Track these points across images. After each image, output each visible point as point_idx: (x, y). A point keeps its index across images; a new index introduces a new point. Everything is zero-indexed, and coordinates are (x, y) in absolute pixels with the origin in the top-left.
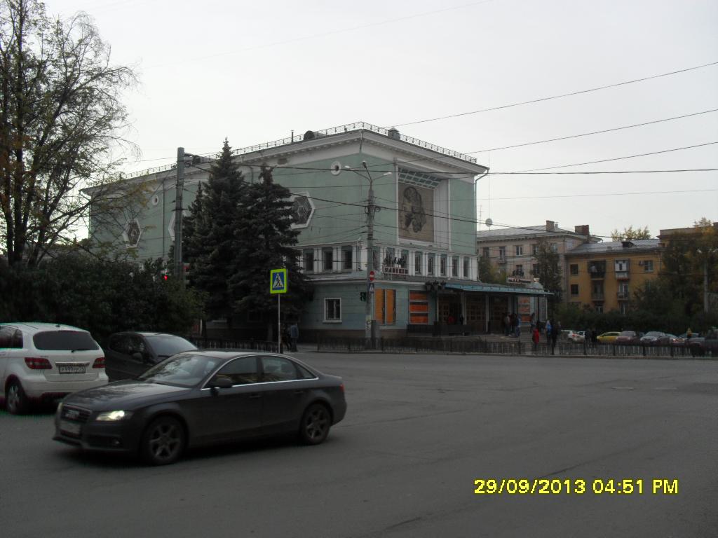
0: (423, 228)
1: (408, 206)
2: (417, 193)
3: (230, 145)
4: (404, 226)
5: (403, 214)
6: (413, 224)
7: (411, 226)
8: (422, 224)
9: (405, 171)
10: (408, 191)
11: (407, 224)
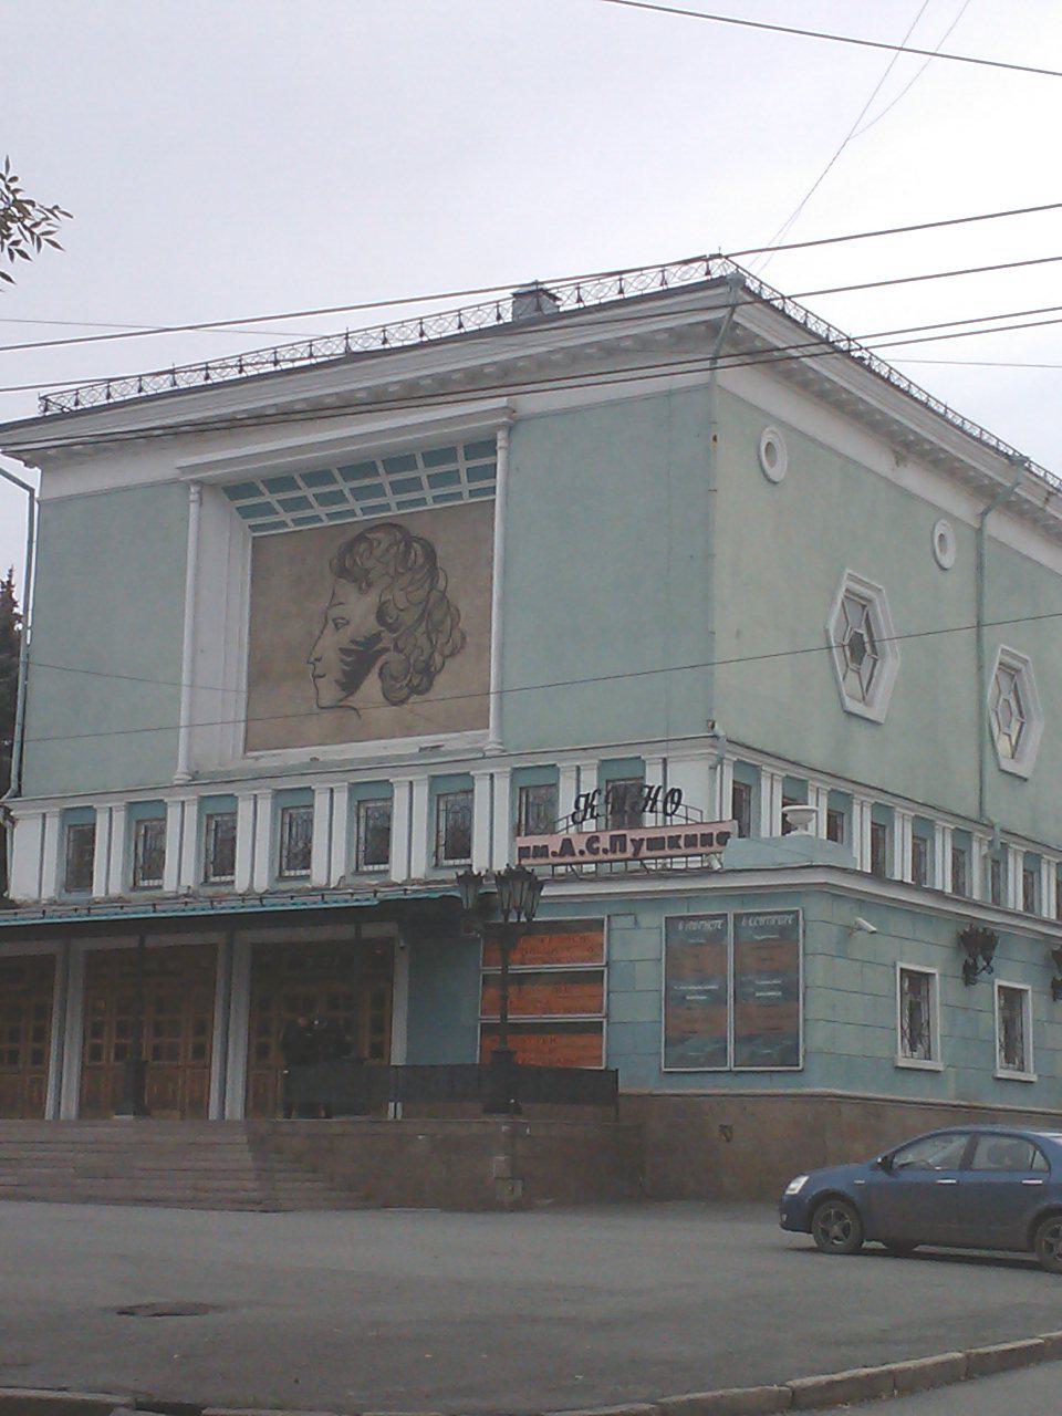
0: (440, 681)
1: (360, 610)
2: (408, 539)
3: (13, 583)
4: (329, 693)
5: (330, 646)
7: (372, 686)
8: (438, 658)
9: (280, 482)
10: (363, 546)
11: (351, 683)
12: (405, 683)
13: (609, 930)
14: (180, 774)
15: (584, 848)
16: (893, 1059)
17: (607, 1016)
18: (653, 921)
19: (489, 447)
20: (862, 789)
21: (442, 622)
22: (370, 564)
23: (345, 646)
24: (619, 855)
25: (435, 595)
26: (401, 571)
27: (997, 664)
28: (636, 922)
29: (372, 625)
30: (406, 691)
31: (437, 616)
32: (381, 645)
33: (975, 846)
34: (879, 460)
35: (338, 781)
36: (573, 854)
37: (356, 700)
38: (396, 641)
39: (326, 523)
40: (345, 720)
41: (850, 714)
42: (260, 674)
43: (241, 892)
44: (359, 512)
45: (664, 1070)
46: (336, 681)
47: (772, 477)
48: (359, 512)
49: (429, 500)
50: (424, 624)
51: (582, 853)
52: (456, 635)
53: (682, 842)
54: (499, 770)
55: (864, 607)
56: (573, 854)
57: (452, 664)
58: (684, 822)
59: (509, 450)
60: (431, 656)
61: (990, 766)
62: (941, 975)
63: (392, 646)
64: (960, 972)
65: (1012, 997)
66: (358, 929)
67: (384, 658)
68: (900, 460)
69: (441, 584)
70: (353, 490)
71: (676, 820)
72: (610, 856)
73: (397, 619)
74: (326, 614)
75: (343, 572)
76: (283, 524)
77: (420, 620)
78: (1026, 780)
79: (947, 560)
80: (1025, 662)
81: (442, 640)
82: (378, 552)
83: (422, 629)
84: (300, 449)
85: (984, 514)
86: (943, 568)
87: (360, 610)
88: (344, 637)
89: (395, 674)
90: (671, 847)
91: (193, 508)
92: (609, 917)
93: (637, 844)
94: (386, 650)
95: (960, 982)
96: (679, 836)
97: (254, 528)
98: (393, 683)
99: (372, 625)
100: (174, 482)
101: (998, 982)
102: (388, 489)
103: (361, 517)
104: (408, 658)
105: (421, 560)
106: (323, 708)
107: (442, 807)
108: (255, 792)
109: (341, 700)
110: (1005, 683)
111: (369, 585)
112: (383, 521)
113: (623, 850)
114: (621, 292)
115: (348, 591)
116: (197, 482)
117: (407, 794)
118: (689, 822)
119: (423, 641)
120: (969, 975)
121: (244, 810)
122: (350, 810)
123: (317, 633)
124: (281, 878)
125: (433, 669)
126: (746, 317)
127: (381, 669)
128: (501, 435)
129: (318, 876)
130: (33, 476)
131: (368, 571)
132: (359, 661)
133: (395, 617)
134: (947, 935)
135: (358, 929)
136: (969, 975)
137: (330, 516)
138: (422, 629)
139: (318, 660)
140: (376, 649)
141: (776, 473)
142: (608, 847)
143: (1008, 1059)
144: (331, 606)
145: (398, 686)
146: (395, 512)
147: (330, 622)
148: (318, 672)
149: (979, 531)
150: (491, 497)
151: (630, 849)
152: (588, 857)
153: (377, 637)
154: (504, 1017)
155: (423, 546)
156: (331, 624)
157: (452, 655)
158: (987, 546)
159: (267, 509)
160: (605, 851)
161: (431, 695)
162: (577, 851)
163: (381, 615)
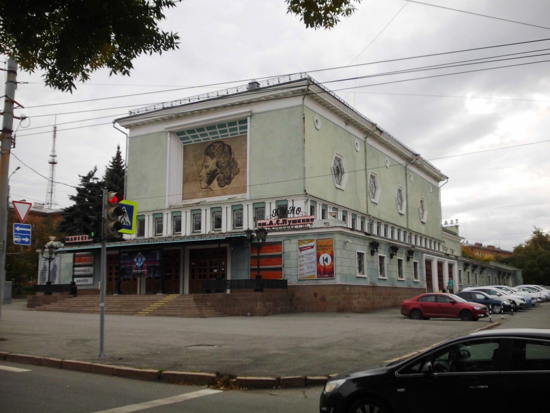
0: (233, 181)
1: (211, 163)
2: (224, 145)
4: (204, 185)
5: (204, 172)
6: (217, 180)
7: (215, 182)
8: (232, 175)
9: (191, 131)
10: (212, 147)
11: (210, 182)
12: (224, 182)
13: (283, 244)
14: (167, 206)
15: (276, 223)
16: (397, 278)
17: (283, 266)
18: (295, 241)
19: (245, 121)
20: (340, 207)
21: (233, 166)
22: (214, 151)
23: (208, 173)
24: (285, 225)
25: (231, 159)
26: (222, 153)
27: (370, 176)
28: (291, 242)
29: (215, 167)
30: (224, 184)
31: (232, 164)
32: (217, 172)
33: (366, 221)
34: (342, 124)
35: (207, 207)
36: (273, 225)
37: (211, 186)
38: (221, 171)
39: (203, 141)
40: (209, 192)
41: (337, 188)
42: (186, 180)
43: (182, 236)
44: (211, 138)
45: (298, 279)
46: (206, 182)
47: (318, 128)
48: (211, 138)
49: (229, 135)
50: (228, 166)
51: (275, 224)
52: (237, 170)
53: (301, 221)
54: (250, 203)
55: (339, 161)
56: (273, 225)
57: (236, 177)
58: (301, 216)
59: (250, 122)
60: (230, 175)
61: (369, 202)
62: (366, 253)
63: (220, 172)
64: (370, 253)
65: (382, 258)
66: (219, 246)
67: (218, 175)
68: (347, 124)
69: (233, 156)
70: (209, 133)
71: (299, 215)
72: (282, 225)
73: (221, 165)
74: (203, 165)
75: (207, 154)
76: (191, 142)
77: (227, 165)
78: (376, 204)
79: (358, 149)
80: (376, 174)
81: (233, 170)
82: (216, 149)
83: (228, 168)
84: (208, 120)
85: (366, 138)
86: (357, 151)
87: (211, 163)
88: (208, 170)
89: (221, 179)
90: (298, 222)
91: (169, 138)
92: (283, 240)
93: (290, 222)
94: (218, 173)
95: (370, 255)
96: (300, 220)
97: (184, 143)
98: (221, 182)
99: (215, 167)
100: (164, 131)
101: (379, 255)
102: (219, 132)
103: (211, 140)
104: (224, 175)
105: (227, 150)
106: (202, 188)
107: (235, 213)
108: (186, 210)
109: (207, 186)
110: (371, 180)
111: (214, 157)
112: (216, 141)
113: (286, 223)
114: (279, 82)
115: (209, 158)
116: (170, 132)
117: (226, 210)
118: (303, 216)
119: (228, 171)
120: (372, 253)
121: (183, 215)
122: (211, 214)
123: (201, 169)
124: (193, 232)
125: (231, 178)
126: (312, 88)
127: (218, 178)
128: (248, 119)
129: (203, 231)
130: (127, 131)
131: (214, 153)
132: (211, 177)
133: (221, 165)
134: (367, 243)
135: (219, 246)
136: (372, 253)
137: (204, 139)
138: (228, 168)
139: (201, 176)
140: (216, 173)
141: (318, 127)
142: (282, 222)
143: (381, 274)
144: (204, 163)
145: (222, 182)
146: (220, 138)
147: (204, 166)
148: (201, 179)
149: (365, 142)
150: (246, 134)
151: (288, 223)
152: (277, 225)
153: (216, 170)
154: (259, 267)
155: (227, 147)
156: (204, 167)
157: (236, 174)
158: (367, 146)
159: (187, 138)
160: (281, 224)
161: (231, 186)
162: (274, 224)
163: (217, 164)
